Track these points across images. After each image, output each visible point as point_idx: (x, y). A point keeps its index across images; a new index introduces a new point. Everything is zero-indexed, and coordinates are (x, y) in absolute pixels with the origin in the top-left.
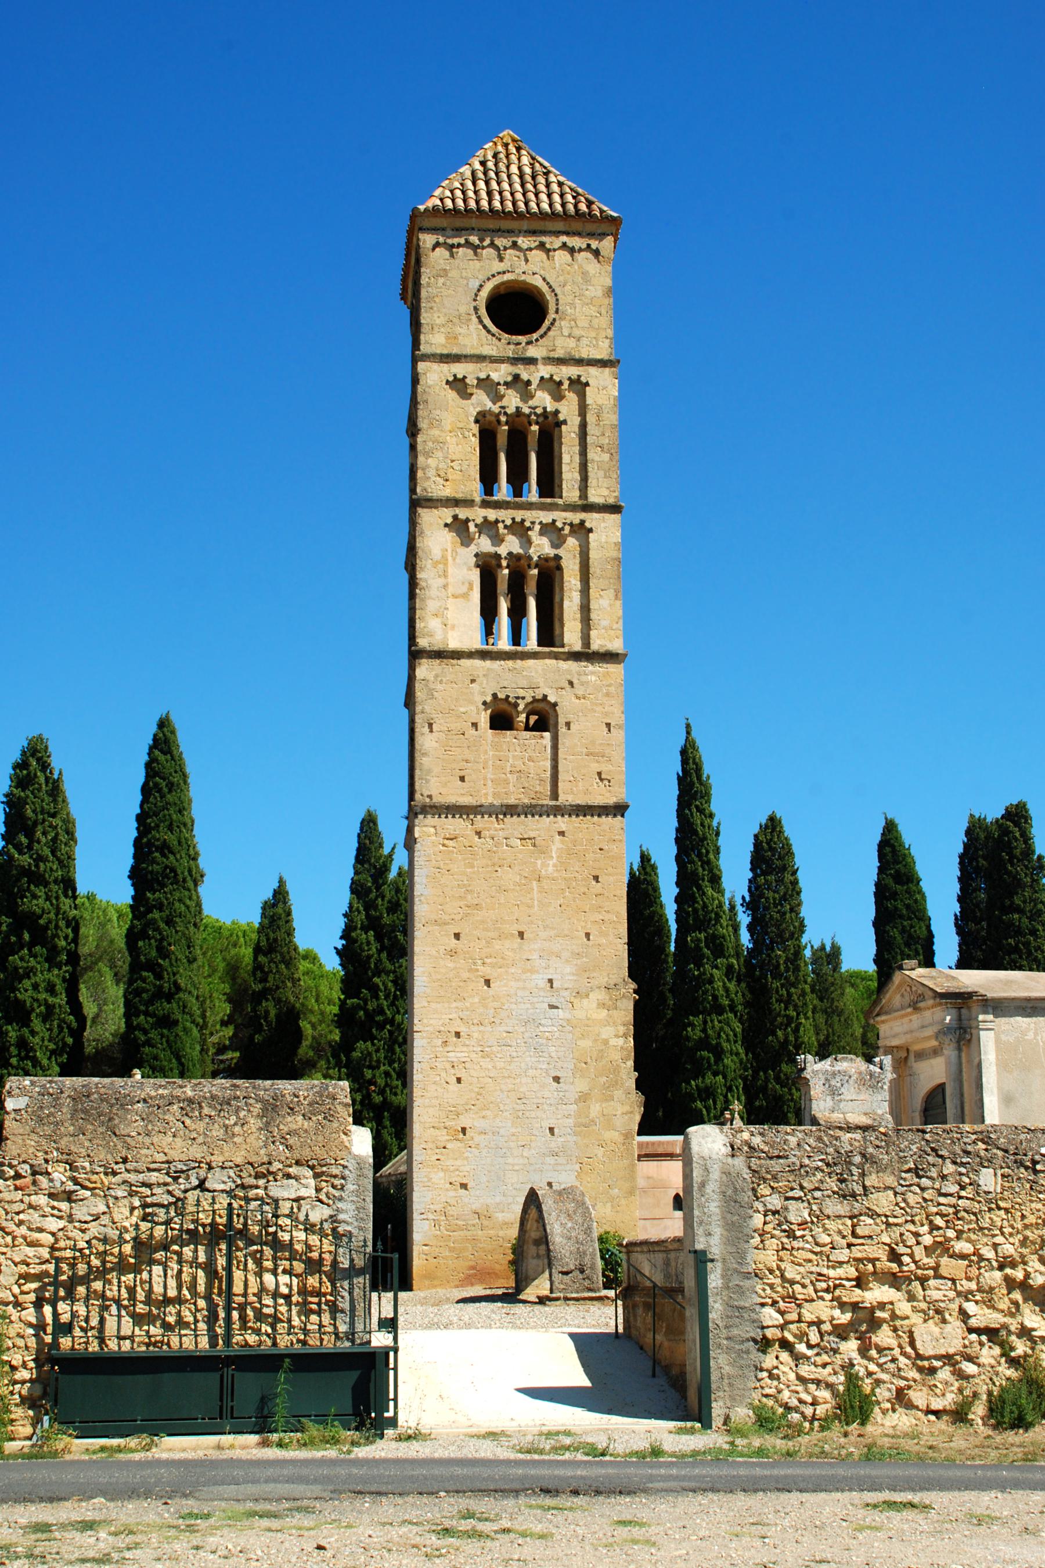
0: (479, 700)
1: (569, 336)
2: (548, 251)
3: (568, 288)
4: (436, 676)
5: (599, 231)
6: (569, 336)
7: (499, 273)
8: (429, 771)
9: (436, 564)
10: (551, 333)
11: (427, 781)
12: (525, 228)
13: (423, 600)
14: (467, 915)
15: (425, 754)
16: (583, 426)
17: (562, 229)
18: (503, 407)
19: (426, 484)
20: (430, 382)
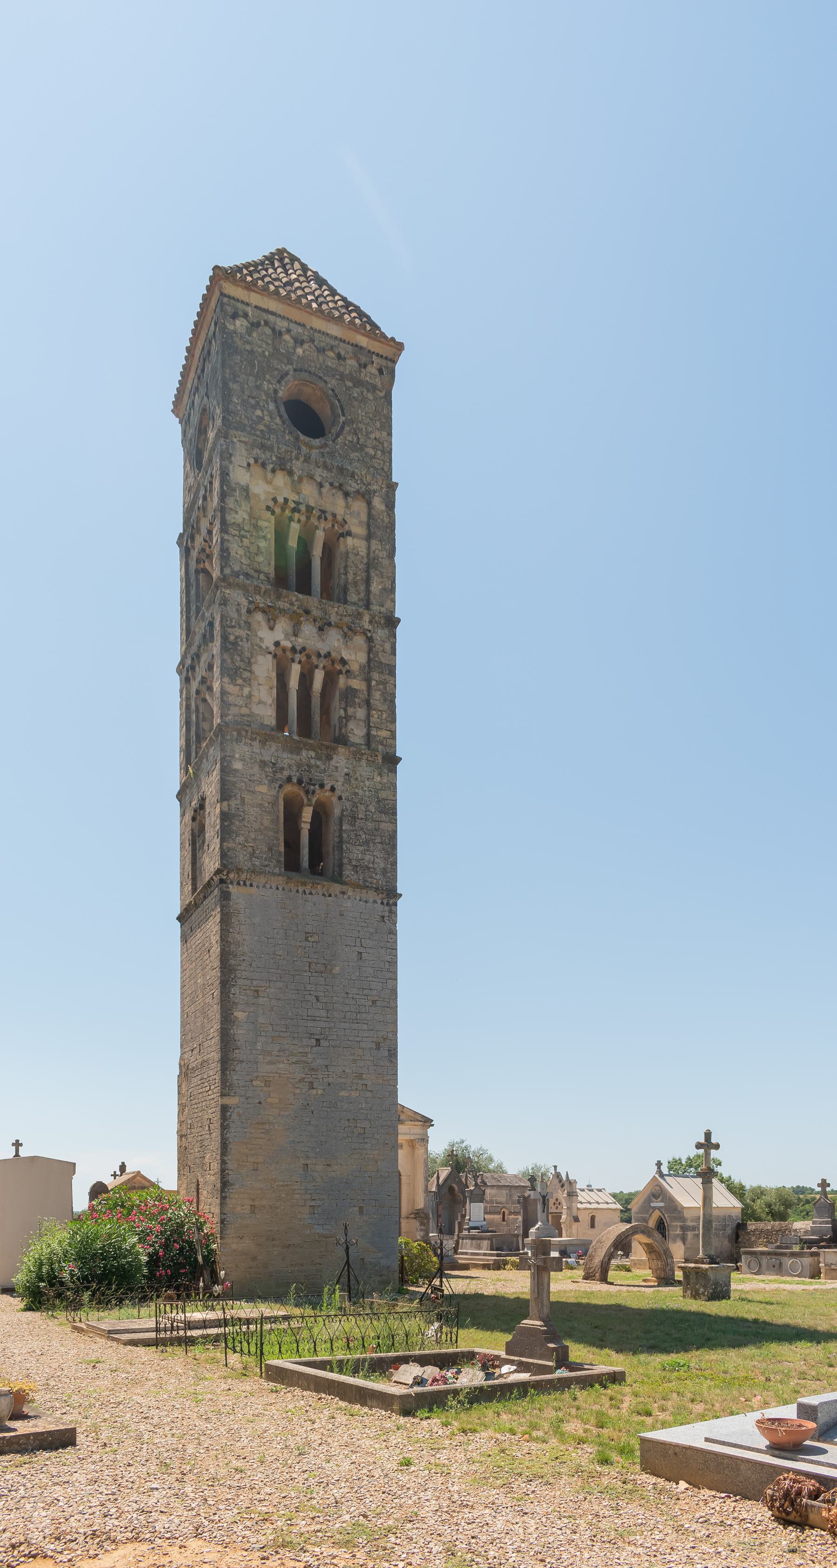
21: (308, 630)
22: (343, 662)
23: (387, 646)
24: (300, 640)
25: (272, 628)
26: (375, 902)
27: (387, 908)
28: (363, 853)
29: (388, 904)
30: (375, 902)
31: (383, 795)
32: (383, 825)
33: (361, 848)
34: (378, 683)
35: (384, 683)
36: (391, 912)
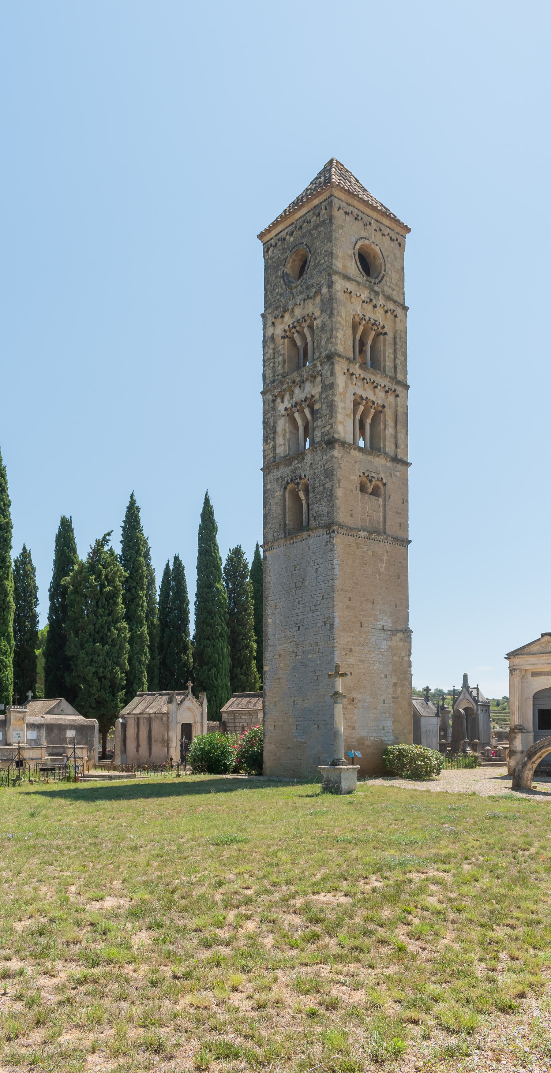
0: (358, 474)
1: (389, 286)
2: (383, 235)
3: (389, 259)
4: (342, 457)
5: (401, 234)
6: (389, 286)
7: (363, 238)
8: (339, 509)
9: (341, 394)
10: (382, 282)
11: (339, 513)
12: (374, 217)
13: (336, 413)
14: (354, 588)
15: (338, 499)
16: (395, 338)
17: (388, 225)
18: (364, 315)
19: (337, 347)
20: (337, 289)
21: (297, 390)
22: (313, 396)
23: (329, 373)
24: (294, 399)
25: (283, 402)
26: (323, 534)
27: (329, 536)
28: (318, 507)
29: (329, 533)
30: (323, 534)
31: (327, 466)
32: (327, 486)
33: (317, 505)
34: (324, 399)
35: (327, 397)
36: (330, 537)
